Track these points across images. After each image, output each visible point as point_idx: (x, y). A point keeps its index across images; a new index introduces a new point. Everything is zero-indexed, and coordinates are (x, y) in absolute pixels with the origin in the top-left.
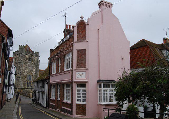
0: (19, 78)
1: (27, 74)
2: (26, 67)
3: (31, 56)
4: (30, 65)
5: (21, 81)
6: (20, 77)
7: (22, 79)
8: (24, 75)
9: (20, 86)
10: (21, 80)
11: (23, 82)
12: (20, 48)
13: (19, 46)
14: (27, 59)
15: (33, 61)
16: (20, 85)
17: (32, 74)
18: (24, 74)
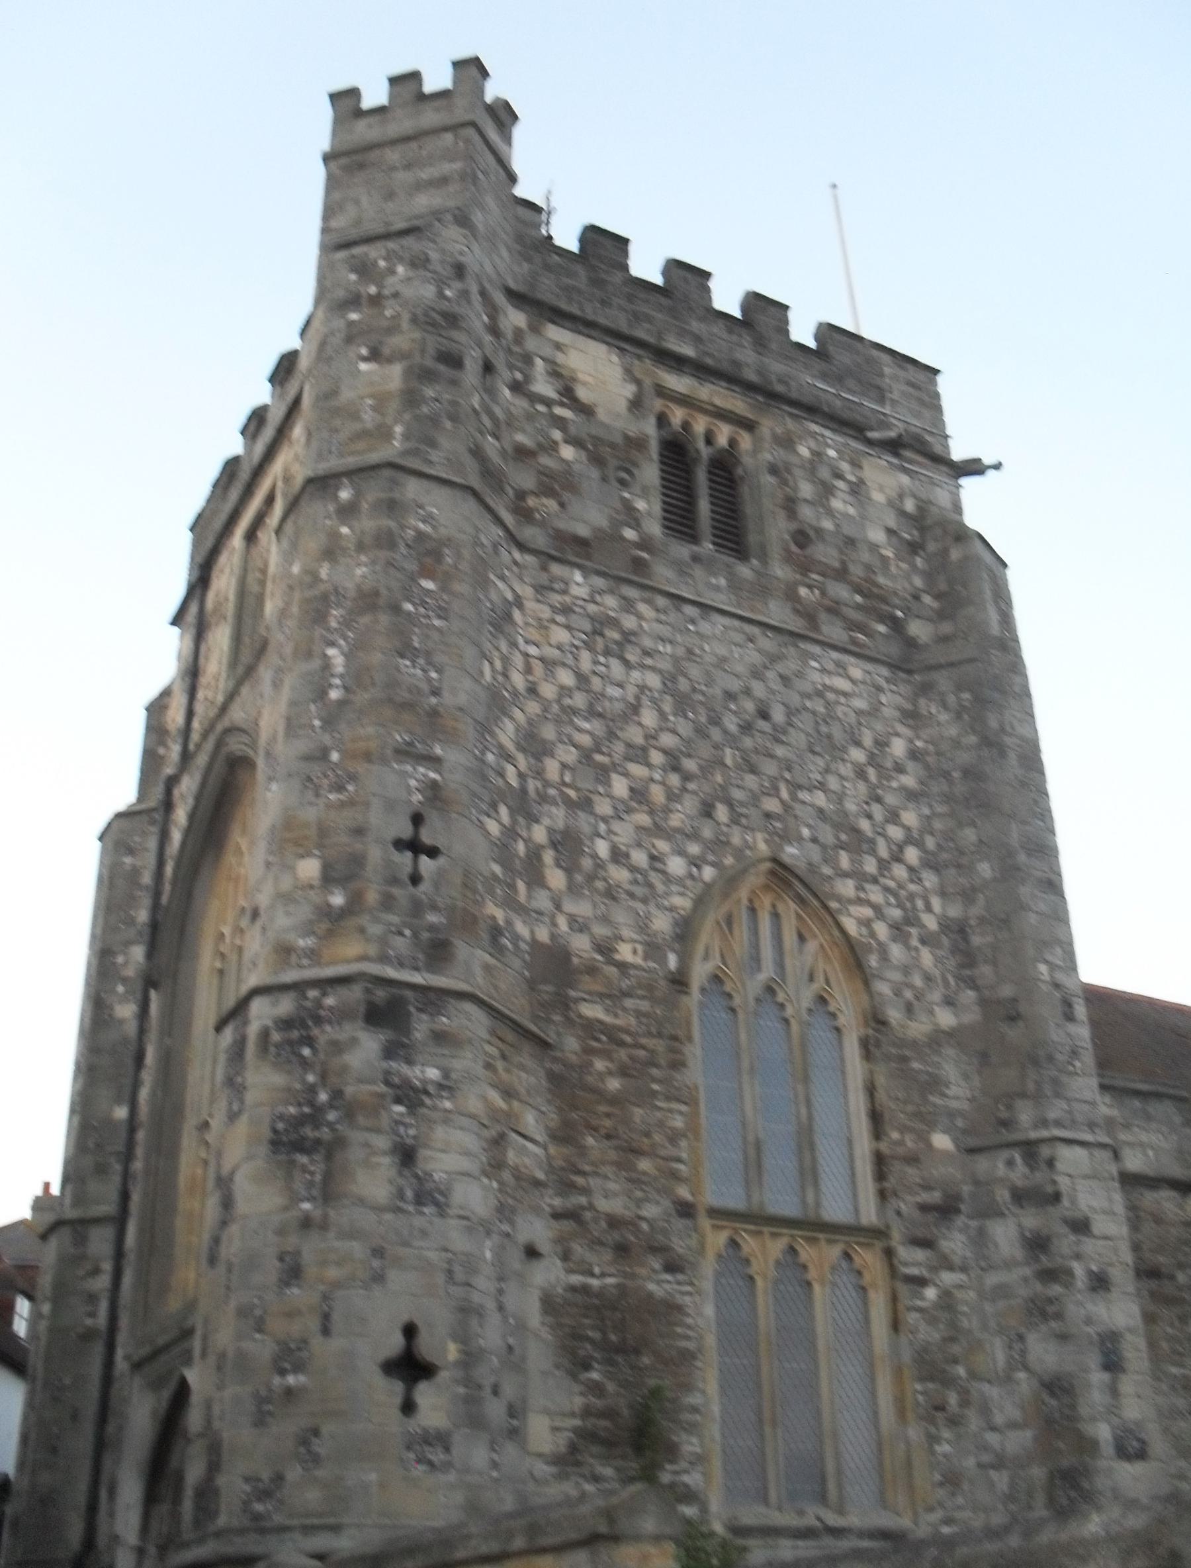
0: (365, 1049)
1: (685, 932)
2: (621, 681)
3: (737, 403)
4: (726, 650)
5: (474, 1197)
6: (387, 1011)
7: (475, 1117)
8: (555, 969)
9: (434, 1404)
10: (452, 1153)
11: (550, 1274)
12: (364, 131)
13: (345, 102)
14: (611, 456)
15: (825, 553)
16: (410, 1367)
17: (854, 957)
18: (555, 913)
